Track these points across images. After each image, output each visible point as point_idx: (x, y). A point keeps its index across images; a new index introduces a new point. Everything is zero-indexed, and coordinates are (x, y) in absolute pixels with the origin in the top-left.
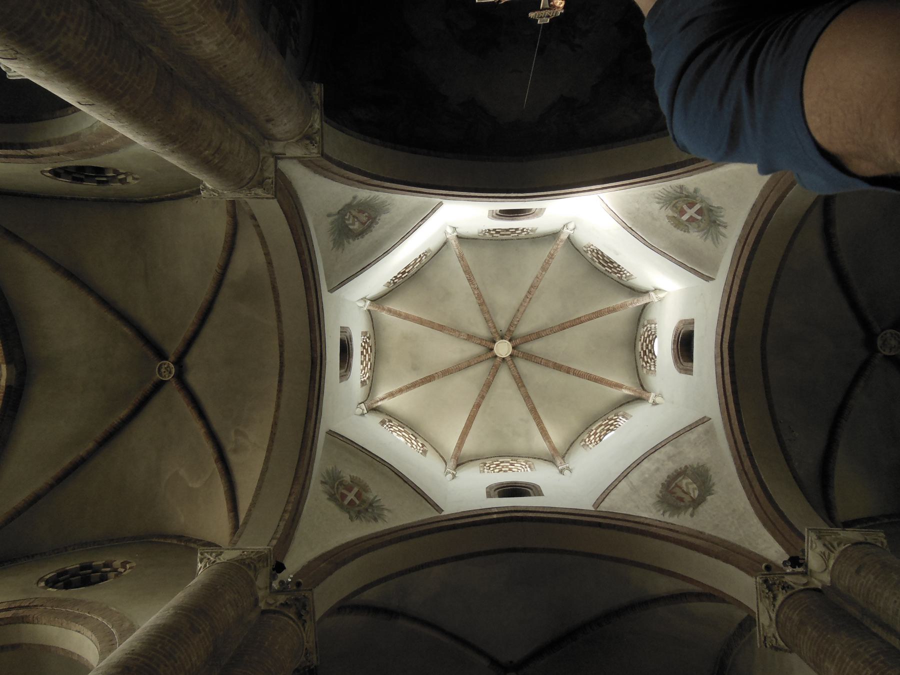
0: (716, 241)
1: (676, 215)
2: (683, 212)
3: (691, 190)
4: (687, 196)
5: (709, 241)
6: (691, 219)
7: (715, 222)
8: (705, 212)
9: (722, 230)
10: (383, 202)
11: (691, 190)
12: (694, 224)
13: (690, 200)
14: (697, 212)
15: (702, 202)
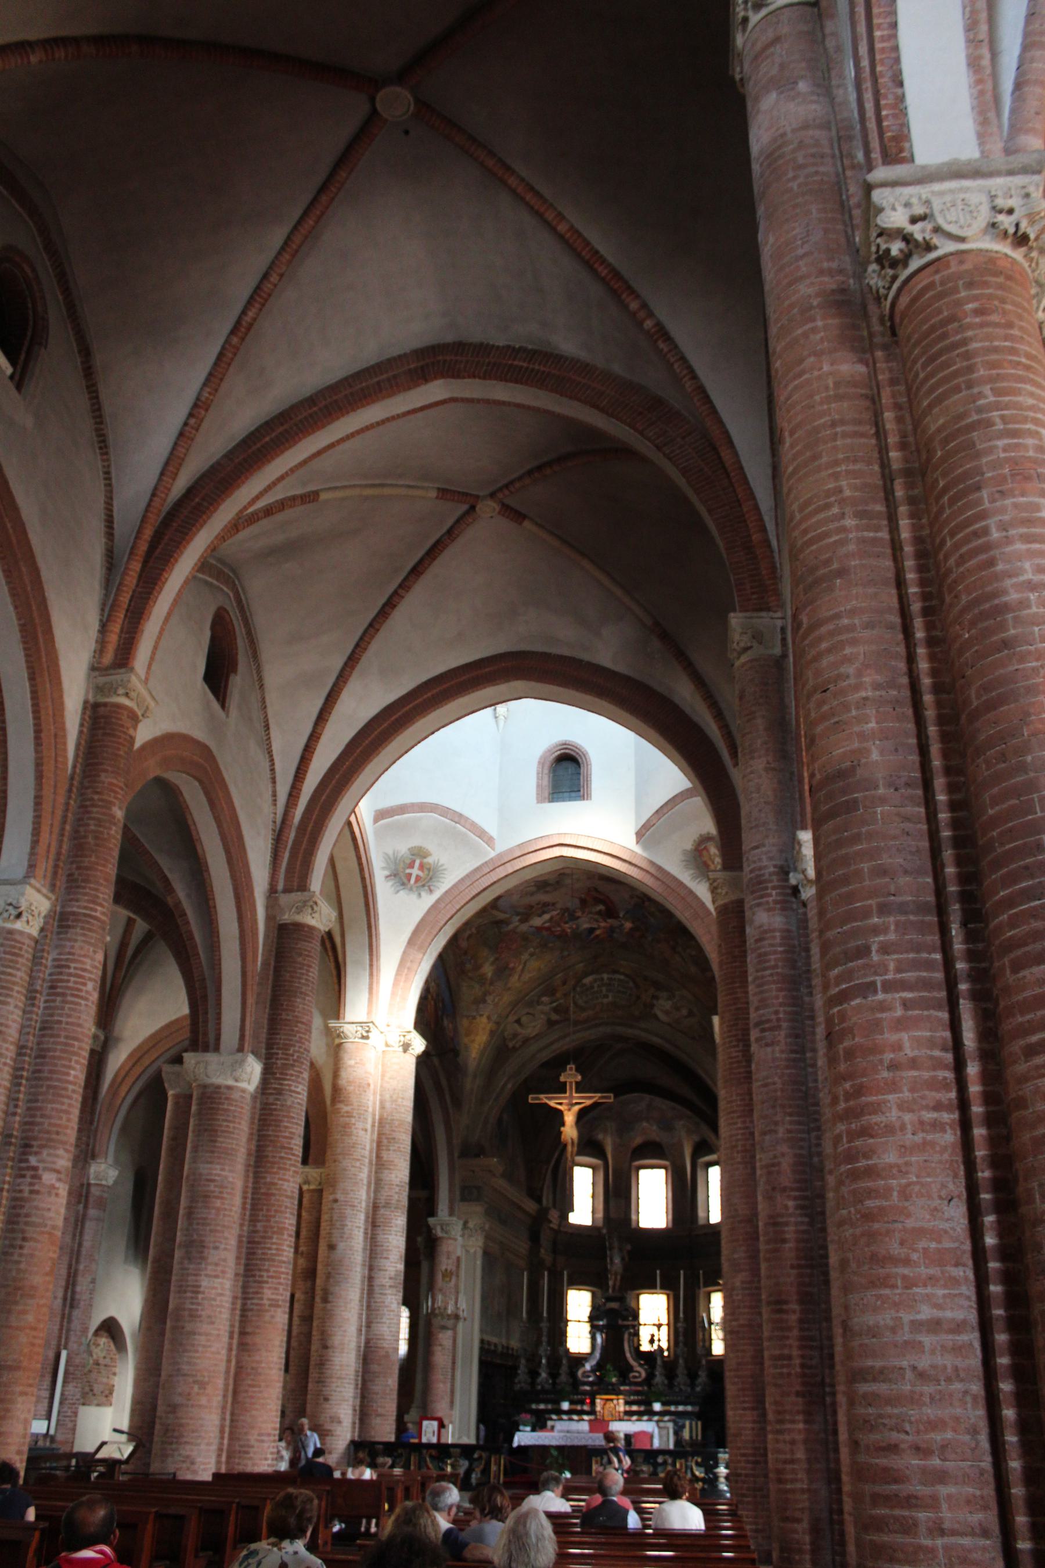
0: (387, 857)
1: (425, 860)
2: (422, 867)
3: (423, 894)
4: (423, 886)
5: (390, 853)
6: (411, 865)
7: (395, 875)
8: (405, 881)
9: (387, 873)
10: (687, 867)
11: (423, 894)
12: (408, 861)
13: (420, 884)
14: (410, 875)
15: (411, 889)
